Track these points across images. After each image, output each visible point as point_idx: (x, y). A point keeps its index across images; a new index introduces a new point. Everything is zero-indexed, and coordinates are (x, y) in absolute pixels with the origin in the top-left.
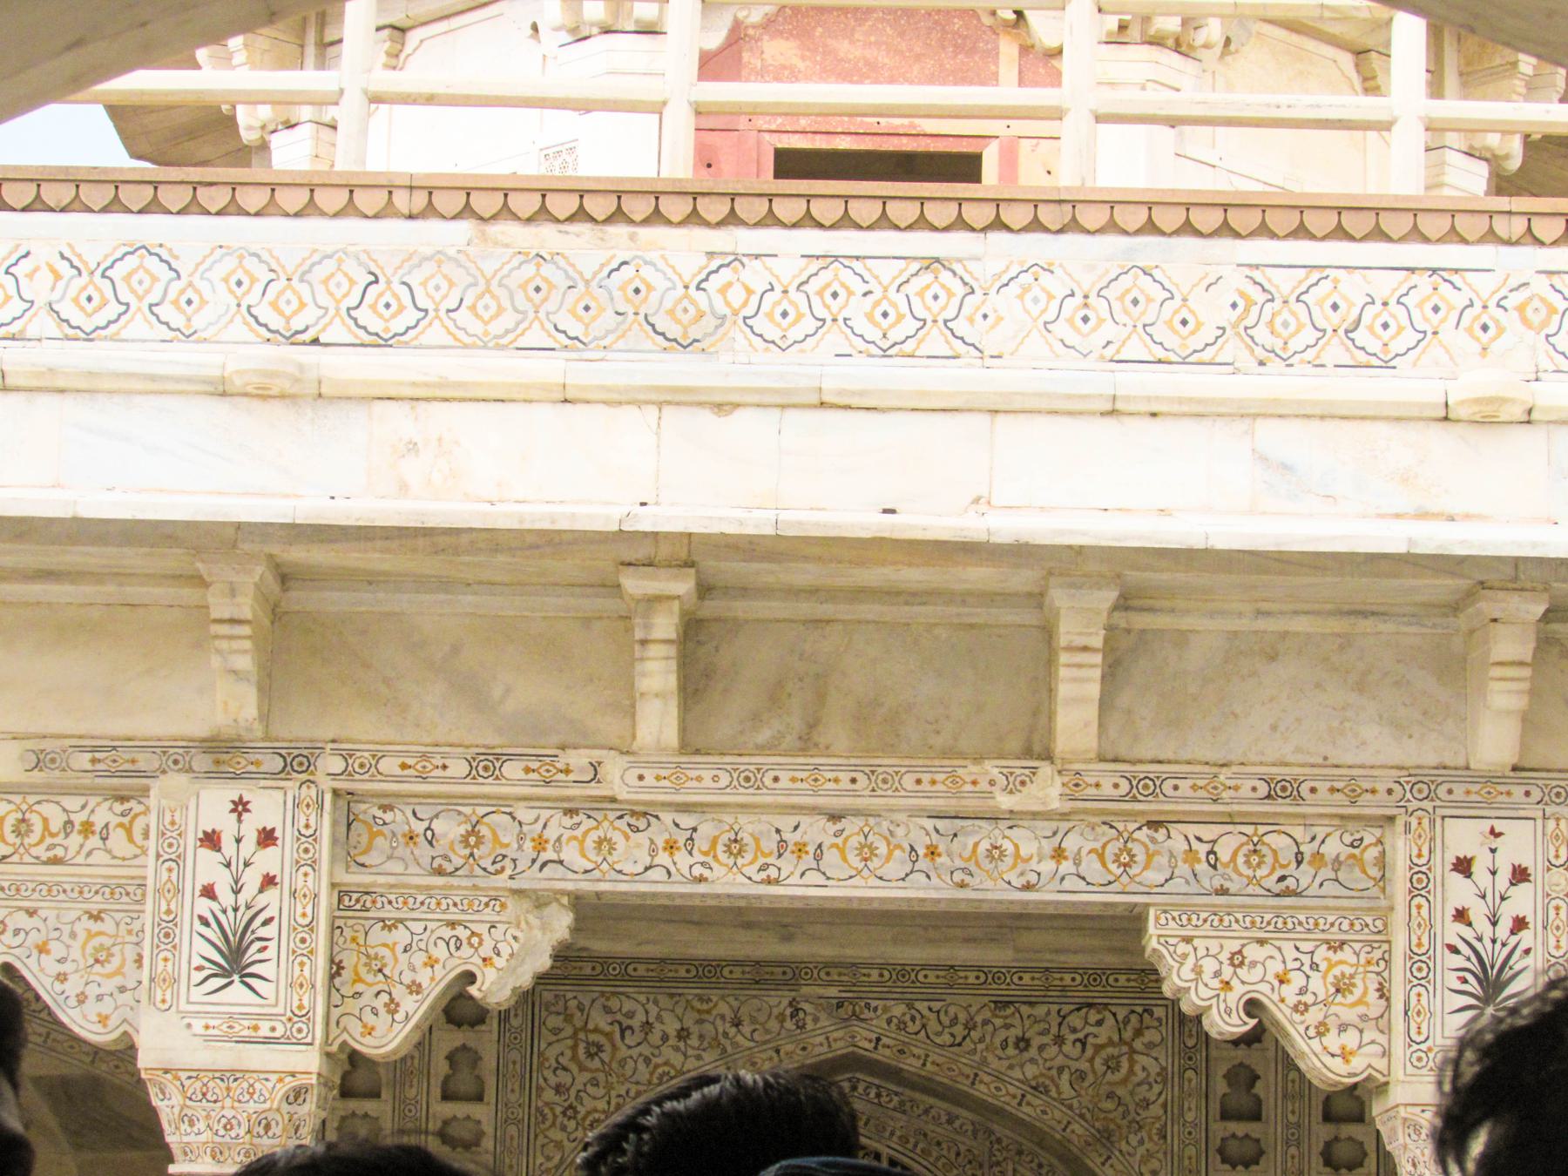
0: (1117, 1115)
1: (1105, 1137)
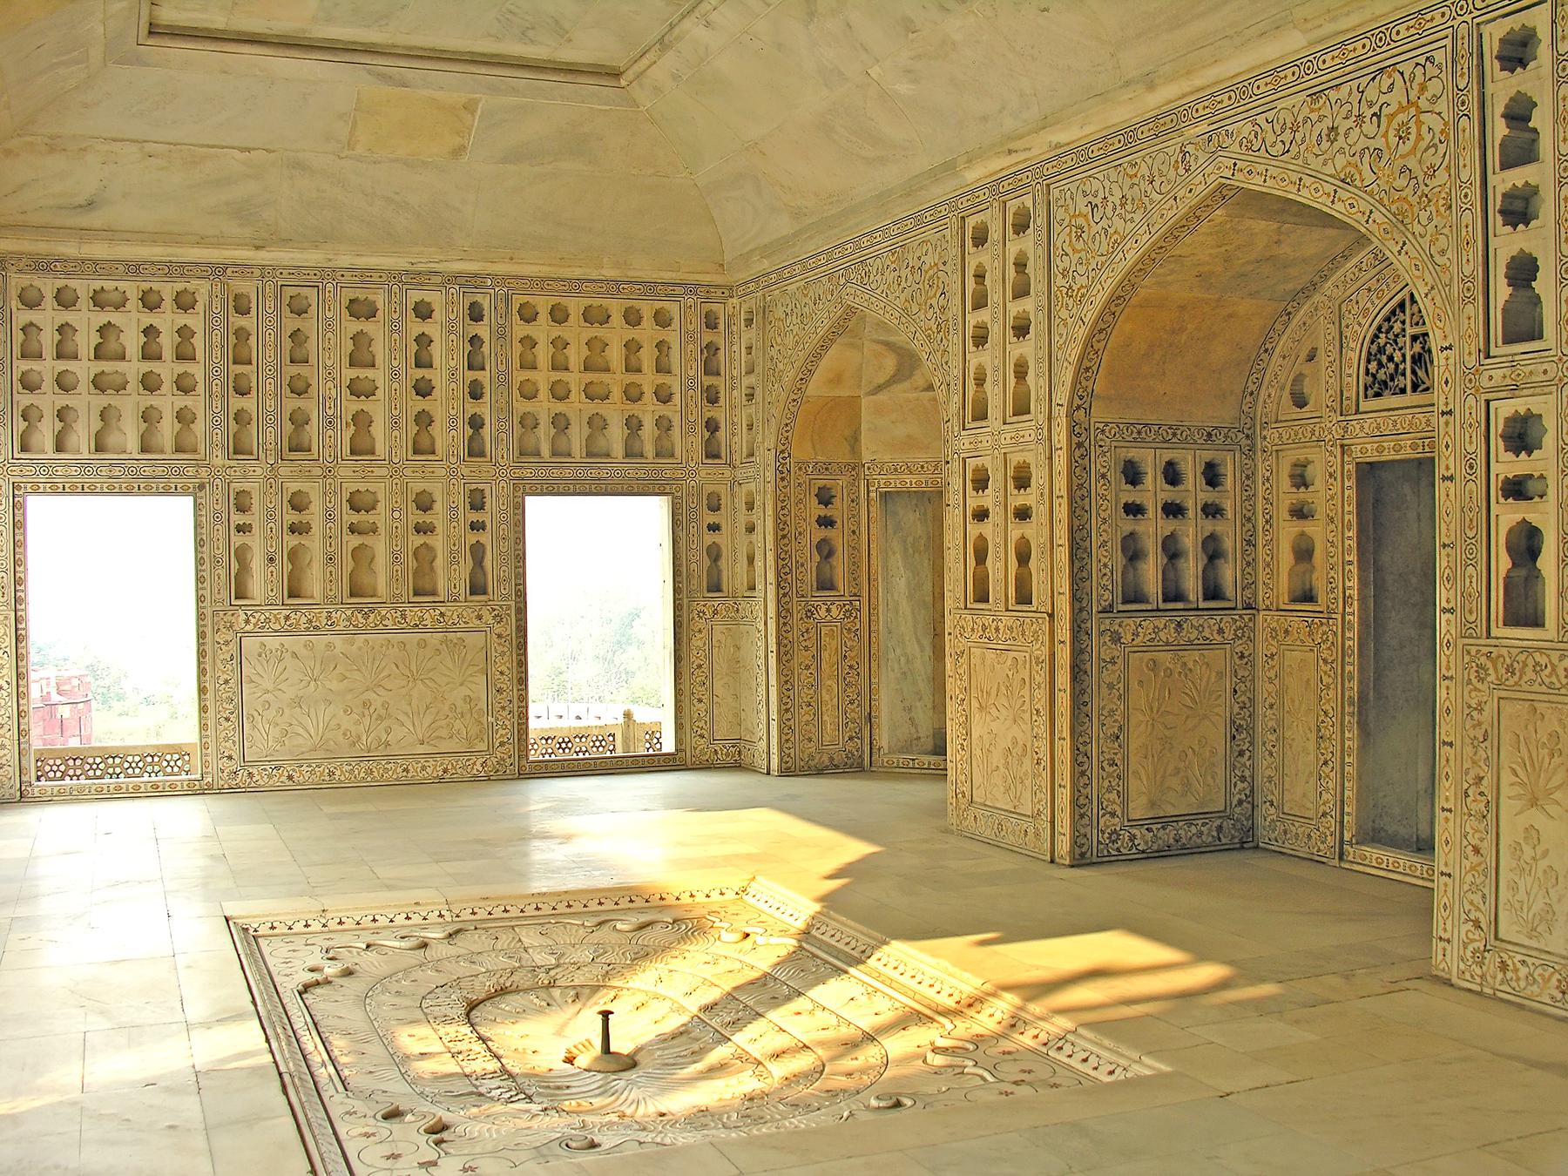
0: (1409, 191)
1: (1400, 219)
